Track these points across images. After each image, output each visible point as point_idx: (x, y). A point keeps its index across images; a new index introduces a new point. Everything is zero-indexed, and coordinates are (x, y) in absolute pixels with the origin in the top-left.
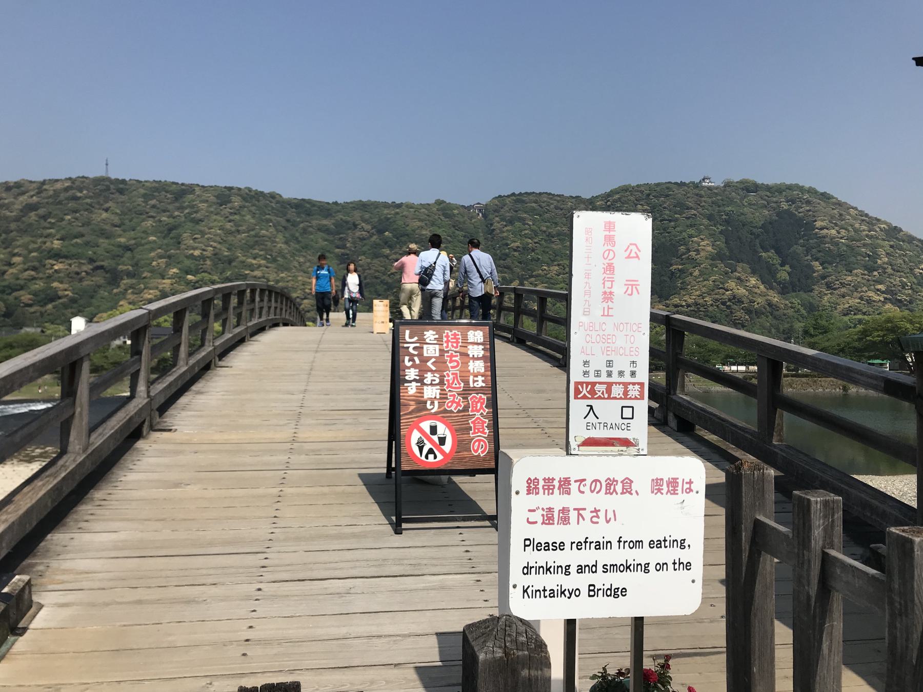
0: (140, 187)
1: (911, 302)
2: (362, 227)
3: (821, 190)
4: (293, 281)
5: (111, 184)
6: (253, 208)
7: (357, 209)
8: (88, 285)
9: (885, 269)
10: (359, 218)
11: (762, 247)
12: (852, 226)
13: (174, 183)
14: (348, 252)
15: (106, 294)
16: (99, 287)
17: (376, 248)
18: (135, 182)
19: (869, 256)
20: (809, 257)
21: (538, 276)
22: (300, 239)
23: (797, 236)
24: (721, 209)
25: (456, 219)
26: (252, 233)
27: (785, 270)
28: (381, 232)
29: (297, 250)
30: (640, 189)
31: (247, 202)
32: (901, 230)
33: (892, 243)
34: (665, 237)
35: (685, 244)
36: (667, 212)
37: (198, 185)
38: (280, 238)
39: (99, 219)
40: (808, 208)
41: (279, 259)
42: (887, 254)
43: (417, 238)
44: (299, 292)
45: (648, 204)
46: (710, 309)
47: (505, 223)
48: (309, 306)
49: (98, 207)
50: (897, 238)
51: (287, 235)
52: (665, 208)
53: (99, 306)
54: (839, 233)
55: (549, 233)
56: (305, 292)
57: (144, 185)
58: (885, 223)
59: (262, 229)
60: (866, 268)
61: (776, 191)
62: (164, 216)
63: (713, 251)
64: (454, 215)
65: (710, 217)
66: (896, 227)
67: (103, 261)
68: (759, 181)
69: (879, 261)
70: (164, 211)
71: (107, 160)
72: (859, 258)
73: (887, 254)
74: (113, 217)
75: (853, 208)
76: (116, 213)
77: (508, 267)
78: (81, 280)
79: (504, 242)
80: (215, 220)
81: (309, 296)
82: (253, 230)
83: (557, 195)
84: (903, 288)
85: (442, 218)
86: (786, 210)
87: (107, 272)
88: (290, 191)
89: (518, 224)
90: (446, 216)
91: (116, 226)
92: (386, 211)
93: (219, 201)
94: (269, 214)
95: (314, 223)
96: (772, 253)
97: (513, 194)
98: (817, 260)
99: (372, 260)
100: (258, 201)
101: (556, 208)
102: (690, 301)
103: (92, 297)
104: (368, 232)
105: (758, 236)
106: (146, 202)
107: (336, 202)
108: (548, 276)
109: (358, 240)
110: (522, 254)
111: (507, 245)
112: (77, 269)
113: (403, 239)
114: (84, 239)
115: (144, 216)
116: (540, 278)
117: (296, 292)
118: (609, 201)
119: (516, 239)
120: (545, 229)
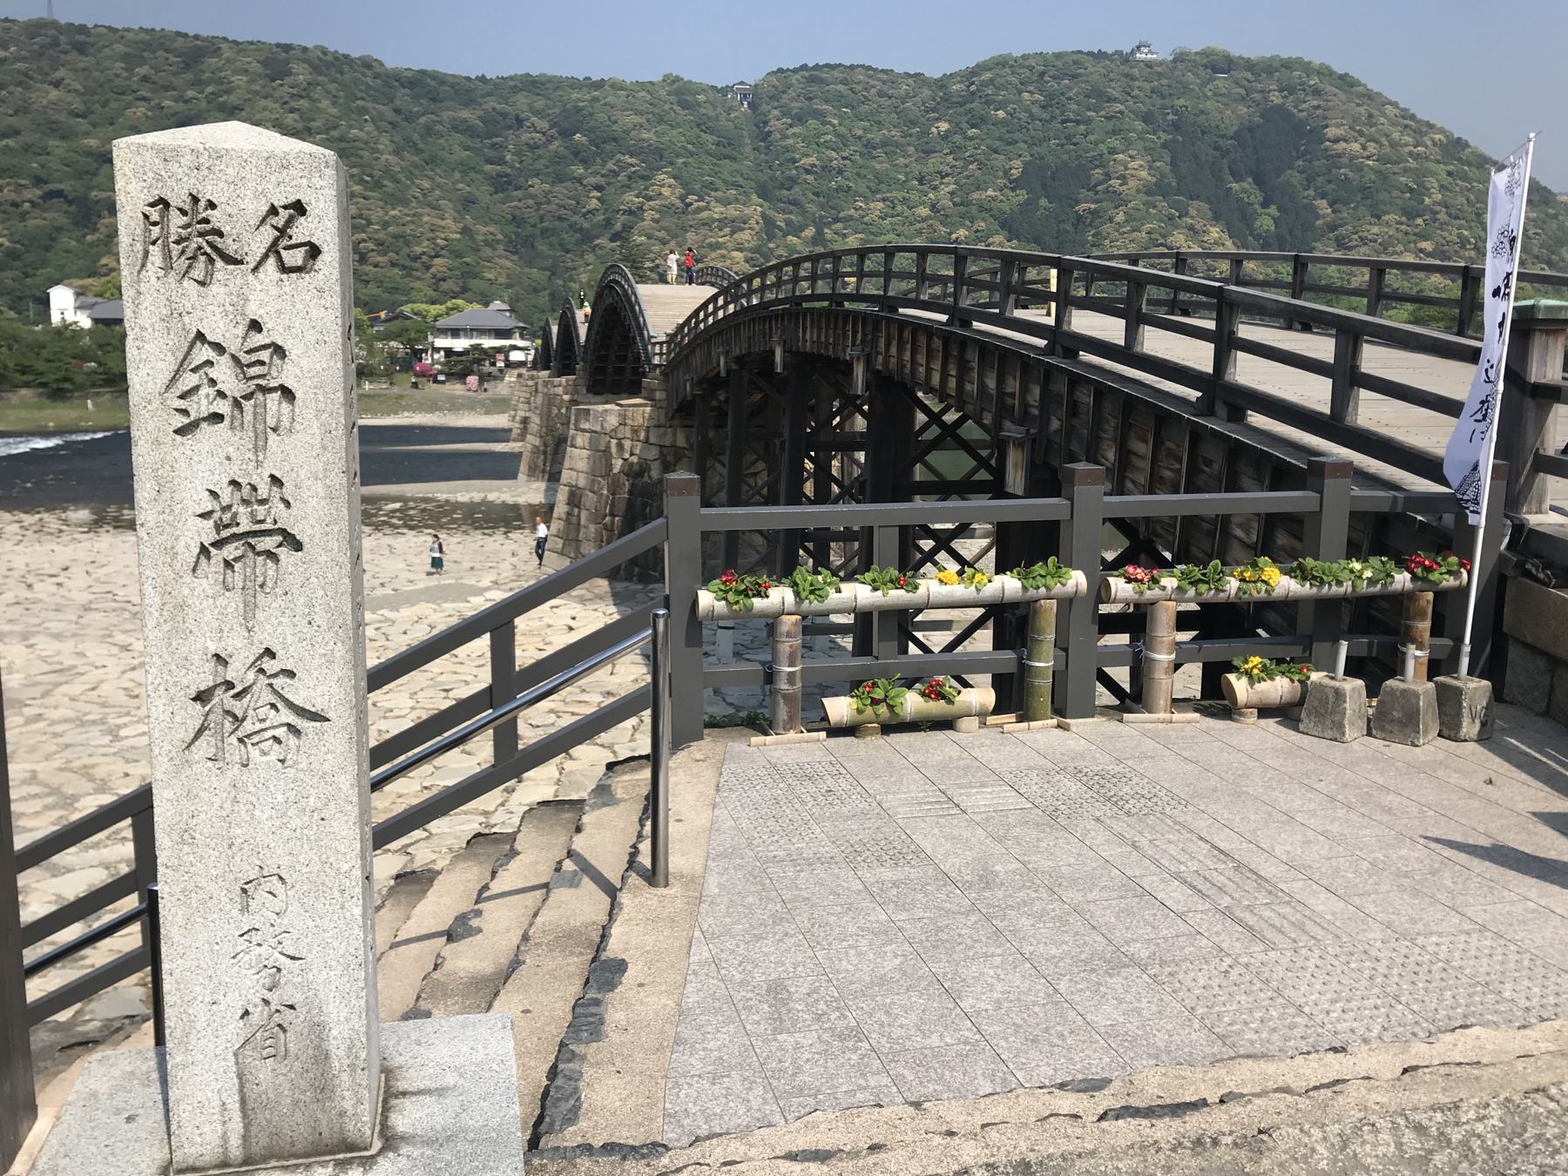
0: (116, 42)
3: (1341, 72)
4: (413, 222)
5: (61, 33)
6: (332, 87)
8: (38, 227)
9: (1436, 213)
10: (525, 108)
11: (1233, 174)
12: (1387, 136)
13: (179, 34)
14: (508, 171)
15: (73, 243)
16: (59, 229)
17: (558, 163)
18: (105, 31)
19: (1411, 190)
20: (1311, 192)
21: (850, 218)
22: (421, 146)
23: (1294, 154)
24: (1167, 101)
25: (703, 111)
26: (335, 133)
27: (1269, 215)
29: (417, 167)
30: (1027, 63)
31: (320, 75)
32: (1467, 145)
33: (1451, 168)
34: (1068, 152)
36: (1074, 107)
37: (225, 39)
38: (384, 143)
39: (45, 102)
40: (1315, 103)
41: (385, 182)
42: (1442, 186)
43: (634, 145)
44: (426, 243)
45: (1041, 91)
47: (789, 121)
48: (445, 269)
49: (40, 77)
50: (1460, 160)
51: (397, 139)
52: (1070, 99)
53: (62, 267)
54: (1364, 148)
55: (868, 141)
56: (436, 245)
57: (122, 37)
58: (1442, 131)
59: (351, 127)
61: (1264, 70)
62: (167, 99)
63: (1149, 178)
64: (699, 105)
65: (1147, 118)
66: (1459, 139)
67: (60, 182)
68: (1236, 51)
69: (1427, 201)
70: (167, 88)
72: (1395, 193)
73: (1442, 186)
74: (70, 98)
75: (1390, 103)
76: (76, 91)
77: (795, 203)
78: (23, 217)
79: (789, 155)
80: (264, 109)
81: (444, 252)
82: (335, 128)
83: (882, 71)
84: (1463, 247)
85: (676, 108)
86: (1277, 106)
87: (70, 203)
88: (399, 56)
89: (812, 123)
90: (685, 105)
91: (78, 116)
92: (575, 95)
93: (268, 72)
94: (363, 99)
95: (446, 115)
96: (1248, 184)
97: (804, 67)
99: (553, 184)
100: (342, 73)
101: (881, 94)
103: (47, 249)
104: (544, 134)
105: (1228, 151)
106: (129, 70)
108: (866, 219)
109: (525, 148)
110: (821, 177)
111: (794, 161)
112: (13, 196)
113: (608, 147)
114: (20, 138)
115: (129, 98)
116: (851, 223)
117: (419, 244)
118: (973, 83)
119: (811, 152)
120: (860, 132)
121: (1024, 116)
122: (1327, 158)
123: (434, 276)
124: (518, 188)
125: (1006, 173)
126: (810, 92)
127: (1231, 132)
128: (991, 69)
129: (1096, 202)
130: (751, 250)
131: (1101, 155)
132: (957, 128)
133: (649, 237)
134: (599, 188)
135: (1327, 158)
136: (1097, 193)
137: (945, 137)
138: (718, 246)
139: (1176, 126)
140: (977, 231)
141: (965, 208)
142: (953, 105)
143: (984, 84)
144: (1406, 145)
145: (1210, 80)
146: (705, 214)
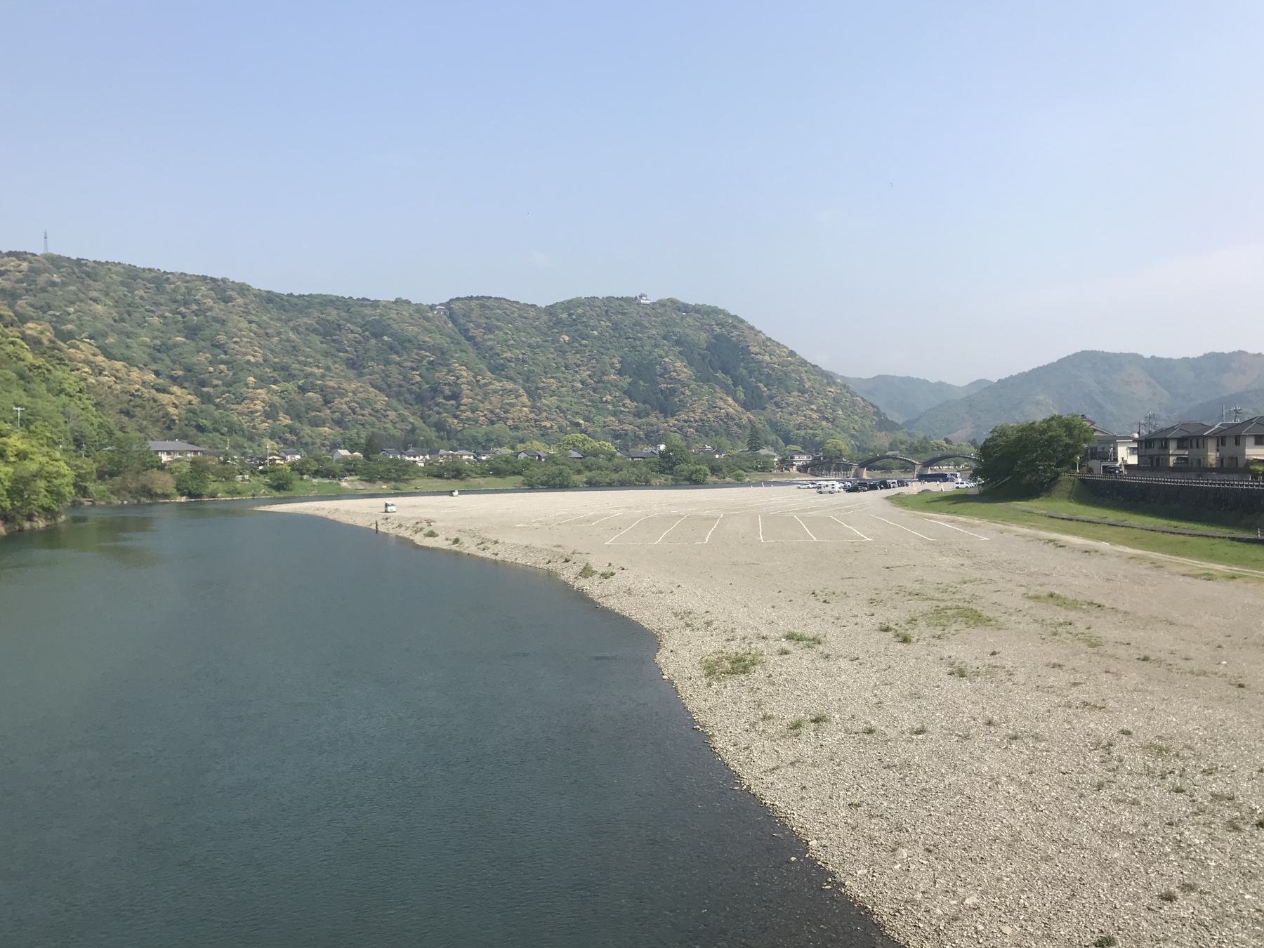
1: (834, 420)
2: (349, 328)
7: (326, 306)
9: (812, 392)
14: (352, 356)
20: (753, 379)
21: (542, 388)
24: (669, 328)
28: (375, 335)
34: (635, 355)
35: (657, 364)
40: (737, 333)
45: (609, 320)
46: (713, 424)
47: (483, 330)
52: (625, 326)
54: (771, 359)
55: (530, 344)
58: (785, 347)
60: (799, 391)
65: (665, 338)
69: (807, 386)
71: (45, 233)
72: (793, 382)
83: (514, 302)
84: (826, 408)
99: (385, 366)
101: (520, 316)
102: (697, 418)
104: (359, 334)
107: (291, 294)
111: (499, 355)
118: (572, 314)
120: (524, 339)
121: (607, 334)
123: (392, 421)
124: (364, 368)
125: (612, 365)
126: (487, 314)
128: (579, 307)
129: (670, 384)
130: (530, 407)
131: (656, 358)
132: (574, 340)
133: (474, 399)
134: (413, 369)
137: (569, 344)
138: (512, 405)
139: (678, 343)
140: (615, 397)
142: (565, 325)
143: (580, 316)
145: (683, 318)
146: (492, 387)
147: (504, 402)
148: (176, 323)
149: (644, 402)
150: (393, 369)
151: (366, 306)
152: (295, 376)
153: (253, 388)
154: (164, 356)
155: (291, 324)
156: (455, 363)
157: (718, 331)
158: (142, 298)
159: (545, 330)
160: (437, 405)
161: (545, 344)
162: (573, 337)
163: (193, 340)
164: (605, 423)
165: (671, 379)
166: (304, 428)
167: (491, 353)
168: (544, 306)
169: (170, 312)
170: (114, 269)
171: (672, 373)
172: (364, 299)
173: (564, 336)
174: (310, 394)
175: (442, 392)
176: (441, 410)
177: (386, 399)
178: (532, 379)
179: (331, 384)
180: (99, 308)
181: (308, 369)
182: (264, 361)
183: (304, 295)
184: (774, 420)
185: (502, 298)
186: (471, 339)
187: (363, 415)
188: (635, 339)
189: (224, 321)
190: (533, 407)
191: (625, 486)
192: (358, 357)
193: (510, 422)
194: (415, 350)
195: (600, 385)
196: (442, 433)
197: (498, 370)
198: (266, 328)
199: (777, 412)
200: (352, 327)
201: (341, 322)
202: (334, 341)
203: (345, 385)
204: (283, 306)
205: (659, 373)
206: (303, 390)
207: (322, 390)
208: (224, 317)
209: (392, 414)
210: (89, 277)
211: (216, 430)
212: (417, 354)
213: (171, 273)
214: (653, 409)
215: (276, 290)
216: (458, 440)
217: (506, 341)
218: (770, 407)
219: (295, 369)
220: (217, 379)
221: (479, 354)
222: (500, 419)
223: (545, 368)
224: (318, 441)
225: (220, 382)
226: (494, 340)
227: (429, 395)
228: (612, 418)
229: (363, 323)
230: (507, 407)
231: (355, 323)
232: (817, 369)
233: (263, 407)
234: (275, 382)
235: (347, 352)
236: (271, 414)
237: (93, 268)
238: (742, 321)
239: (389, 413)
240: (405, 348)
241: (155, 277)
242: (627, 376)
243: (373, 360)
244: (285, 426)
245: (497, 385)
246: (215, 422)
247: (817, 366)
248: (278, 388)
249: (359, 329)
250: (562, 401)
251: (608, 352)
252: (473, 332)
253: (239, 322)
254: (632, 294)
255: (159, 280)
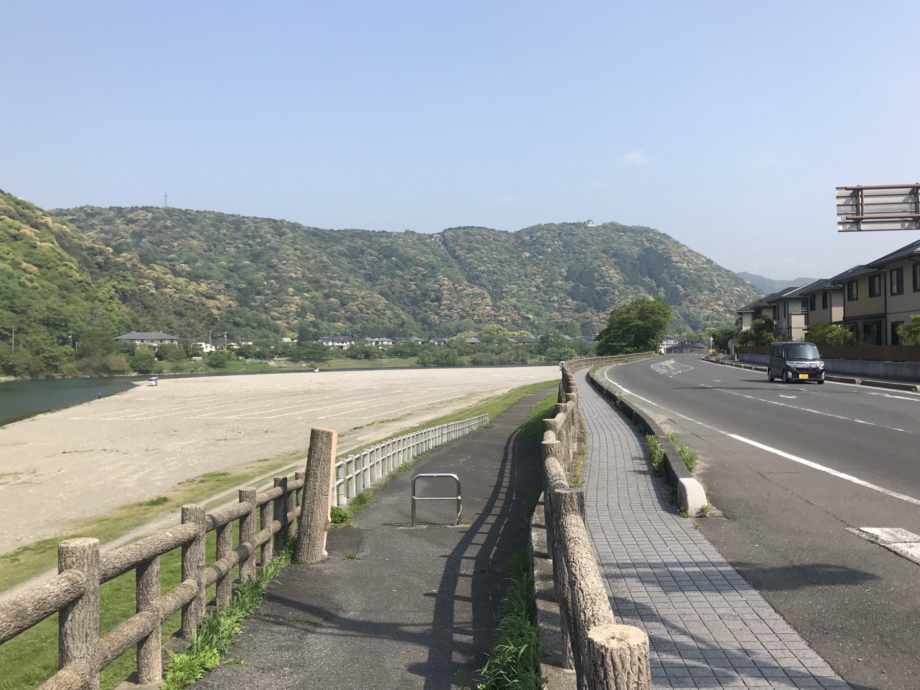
7: (354, 237)
19: (710, 282)
20: (673, 282)
21: (506, 292)
24: (608, 245)
28: (387, 257)
32: (712, 262)
33: (717, 273)
36: (576, 247)
40: (663, 247)
45: (561, 240)
54: (688, 266)
58: (703, 257)
60: (709, 290)
69: (716, 286)
71: (166, 193)
72: (705, 283)
83: (491, 230)
84: (731, 303)
98: (679, 283)
108: (513, 292)
111: (476, 268)
118: (533, 236)
120: (496, 256)
121: (558, 251)
122: (676, 269)
124: (377, 280)
125: (561, 274)
127: (636, 257)
130: (491, 306)
132: (533, 256)
133: (451, 301)
134: (411, 280)
135: (676, 269)
136: (600, 282)
137: (529, 259)
138: (478, 305)
139: (614, 255)
140: (560, 297)
141: (549, 288)
143: (538, 238)
144: (700, 264)
145: (620, 236)
146: (465, 292)
147: (473, 302)
148: (246, 251)
149: (583, 301)
150: (397, 280)
151: (382, 237)
152: (323, 286)
153: (292, 296)
154: (235, 274)
155: (328, 250)
156: (440, 275)
157: (648, 245)
158: (224, 235)
159: (511, 248)
160: (425, 305)
161: (512, 259)
162: (533, 254)
163: (256, 263)
164: (551, 317)
165: (605, 283)
166: (324, 323)
167: (470, 267)
168: (513, 232)
169: (242, 244)
170: (208, 215)
171: (606, 279)
172: (383, 232)
173: (525, 253)
174: (332, 299)
175: (430, 296)
176: (427, 309)
177: (386, 302)
178: (498, 285)
179: (347, 292)
180: (195, 243)
181: (332, 282)
182: (303, 276)
183: (341, 230)
184: (687, 313)
185: (483, 227)
186: (456, 257)
187: (368, 314)
188: (580, 254)
189: (277, 249)
190: (494, 306)
191: (504, 364)
192: (373, 272)
193: (476, 318)
194: (414, 267)
195: (551, 288)
196: (425, 326)
197: (473, 280)
198: (306, 254)
199: (691, 307)
200: (371, 252)
201: (364, 248)
202: (357, 262)
203: (357, 293)
204: (324, 238)
205: (596, 279)
206: (327, 296)
207: (340, 296)
208: (278, 247)
209: (389, 313)
210: (191, 222)
211: (248, 325)
212: (415, 270)
213: (248, 217)
214: (590, 306)
215: (321, 227)
216: (436, 331)
217: (482, 258)
218: (685, 303)
219: (323, 282)
220: (268, 289)
221: (462, 268)
222: (469, 315)
223: (510, 277)
224: (332, 332)
225: (270, 292)
226: (473, 258)
227: (420, 298)
228: (557, 313)
229: (379, 248)
230: (475, 306)
231: (374, 248)
232: (729, 273)
233: (296, 309)
234: (308, 291)
235: (366, 269)
236: (301, 313)
237: (194, 215)
238: (669, 238)
239: (387, 312)
240: (406, 266)
241: (235, 220)
242: (571, 282)
243: (383, 274)
244: (310, 322)
245: (470, 290)
246: (248, 320)
247: (730, 271)
248: (308, 295)
249: (376, 253)
250: (519, 302)
251: (558, 264)
252: (459, 253)
253: (288, 249)
254: (582, 220)
255: (237, 222)
